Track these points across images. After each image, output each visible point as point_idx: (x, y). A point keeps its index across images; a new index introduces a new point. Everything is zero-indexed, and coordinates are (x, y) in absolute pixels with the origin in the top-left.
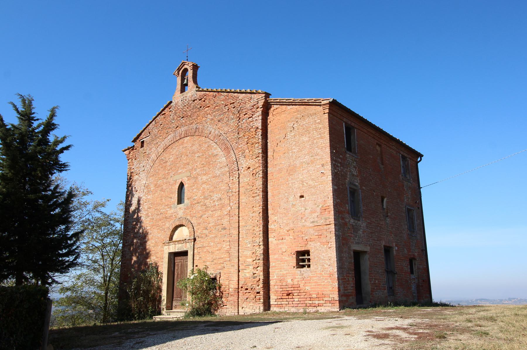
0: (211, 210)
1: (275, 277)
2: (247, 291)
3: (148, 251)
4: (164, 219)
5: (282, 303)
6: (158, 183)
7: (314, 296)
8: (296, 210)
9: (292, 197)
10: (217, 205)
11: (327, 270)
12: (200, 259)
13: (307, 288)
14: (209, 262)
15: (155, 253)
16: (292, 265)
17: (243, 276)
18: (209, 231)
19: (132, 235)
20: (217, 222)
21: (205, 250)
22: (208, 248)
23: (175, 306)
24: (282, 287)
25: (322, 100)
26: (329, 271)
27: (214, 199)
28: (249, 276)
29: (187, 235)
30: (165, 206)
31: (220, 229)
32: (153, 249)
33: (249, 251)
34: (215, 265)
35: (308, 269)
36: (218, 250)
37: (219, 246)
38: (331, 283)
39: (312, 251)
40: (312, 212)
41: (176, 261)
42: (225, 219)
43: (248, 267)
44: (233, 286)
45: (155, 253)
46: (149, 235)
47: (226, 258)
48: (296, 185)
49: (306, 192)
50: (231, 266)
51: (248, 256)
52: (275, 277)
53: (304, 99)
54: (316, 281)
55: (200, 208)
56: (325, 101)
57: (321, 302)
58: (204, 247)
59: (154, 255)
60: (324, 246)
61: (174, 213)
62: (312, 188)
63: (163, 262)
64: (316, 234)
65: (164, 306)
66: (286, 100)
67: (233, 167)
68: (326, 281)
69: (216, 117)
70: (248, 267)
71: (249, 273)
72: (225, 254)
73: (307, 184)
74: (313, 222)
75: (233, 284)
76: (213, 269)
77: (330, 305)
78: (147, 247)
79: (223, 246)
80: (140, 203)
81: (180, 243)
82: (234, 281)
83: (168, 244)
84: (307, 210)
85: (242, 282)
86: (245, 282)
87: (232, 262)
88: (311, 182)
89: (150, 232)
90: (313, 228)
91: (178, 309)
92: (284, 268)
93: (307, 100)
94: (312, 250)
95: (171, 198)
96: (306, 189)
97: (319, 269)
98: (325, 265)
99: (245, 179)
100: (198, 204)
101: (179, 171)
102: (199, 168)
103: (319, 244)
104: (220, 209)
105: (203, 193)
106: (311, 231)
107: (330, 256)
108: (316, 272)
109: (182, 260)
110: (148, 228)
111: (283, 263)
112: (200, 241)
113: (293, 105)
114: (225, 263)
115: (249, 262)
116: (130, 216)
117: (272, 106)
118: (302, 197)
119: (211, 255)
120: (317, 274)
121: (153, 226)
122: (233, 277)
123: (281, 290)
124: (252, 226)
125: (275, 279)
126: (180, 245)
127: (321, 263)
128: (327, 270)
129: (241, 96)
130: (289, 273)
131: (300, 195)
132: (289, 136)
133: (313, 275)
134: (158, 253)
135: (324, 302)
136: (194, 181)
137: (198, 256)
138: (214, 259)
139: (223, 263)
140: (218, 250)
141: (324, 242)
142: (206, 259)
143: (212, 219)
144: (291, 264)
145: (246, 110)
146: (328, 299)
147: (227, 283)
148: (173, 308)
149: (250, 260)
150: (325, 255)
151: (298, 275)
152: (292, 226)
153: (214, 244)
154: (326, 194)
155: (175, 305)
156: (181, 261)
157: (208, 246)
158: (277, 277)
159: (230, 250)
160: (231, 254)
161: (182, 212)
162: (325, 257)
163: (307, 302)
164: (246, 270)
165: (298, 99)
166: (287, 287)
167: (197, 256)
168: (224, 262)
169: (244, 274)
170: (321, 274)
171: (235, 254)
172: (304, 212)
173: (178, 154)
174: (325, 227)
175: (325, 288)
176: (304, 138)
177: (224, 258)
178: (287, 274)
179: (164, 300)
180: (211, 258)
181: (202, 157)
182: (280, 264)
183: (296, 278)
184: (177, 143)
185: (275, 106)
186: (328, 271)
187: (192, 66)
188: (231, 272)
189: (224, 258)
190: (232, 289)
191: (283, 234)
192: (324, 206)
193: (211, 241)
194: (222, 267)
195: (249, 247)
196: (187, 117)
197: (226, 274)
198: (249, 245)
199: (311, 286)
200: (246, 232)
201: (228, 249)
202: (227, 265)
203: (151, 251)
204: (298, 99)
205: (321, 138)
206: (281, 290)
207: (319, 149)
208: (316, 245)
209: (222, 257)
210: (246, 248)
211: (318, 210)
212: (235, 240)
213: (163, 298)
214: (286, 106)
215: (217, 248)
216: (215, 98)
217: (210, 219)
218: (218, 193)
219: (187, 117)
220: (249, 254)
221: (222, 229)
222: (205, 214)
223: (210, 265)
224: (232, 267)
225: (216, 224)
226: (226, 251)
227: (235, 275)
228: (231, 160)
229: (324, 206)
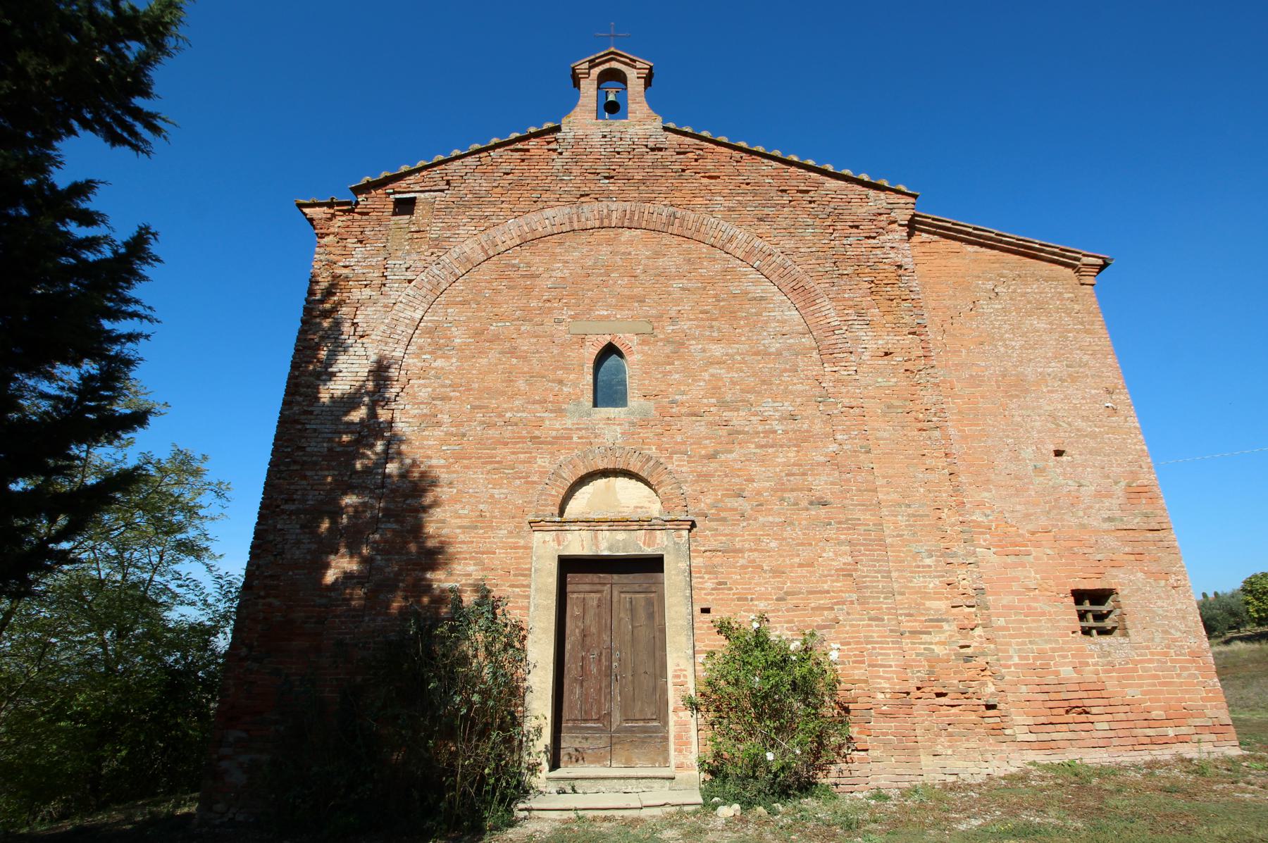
0: (755, 442)
1: (1016, 660)
2: (942, 700)
3: (431, 543)
4: (524, 443)
5: (1055, 736)
6: (492, 328)
7: (1157, 715)
8: (1051, 483)
9: (1030, 450)
10: (780, 432)
11: (1180, 644)
12: (719, 589)
13: (1129, 691)
14: (766, 599)
15: (477, 553)
16: (1067, 628)
17: (922, 654)
18: (755, 504)
19: (329, 479)
20: (789, 481)
21: (741, 562)
22: (756, 554)
23: (574, 753)
24: (1046, 688)
25: (1084, 255)
26: (1188, 648)
27: (766, 414)
28: (948, 655)
29: (637, 507)
30: (528, 403)
31: (804, 503)
32: (461, 537)
33: (930, 577)
34: (794, 611)
35: (1121, 640)
36: (801, 565)
37: (806, 554)
38: (1201, 679)
39: (1125, 592)
40: (1099, 495)
41: (569, 588)
42: (819, 475)
43: (937, 626)
44: (888, 685)
45: (477, 553)
46: (442, 487)
47: (842, 591)
48: (1038, 424)
49: (1072, 444)
50: (870, 619)
51: (930, 593)
52: (1016, 660)
53: (1031, 240)
54: (1154, 672)
55: (702, 429)
56: (1090, 258)
57: (1184, 730)
58: (741, 551)
59: (466, 559)
60: (1158, 583)
61: (580, 429)
62: (1086, 436)
63: (529, 586)
64: (1127, 549)
65: (542, 755)
66: (975, 229)
67: (833, 342)
68: (1185, 674)
69: (748, 209)
70: (937, 626)
71: (943, 643)
72: (837, 581)
73: (1069, 424)
74: (1110, 519)
75: (888, 679)
76: (786, 625)
77: (1213, 737)
78: (430, 529)
79: (824, 555)
80: (388, 379)
81: (623, 528)
82: (891, 666)
83: (560, 528)
84: (1085, 488)
85: (919, 671)
86: (930, 673)
87: (871, 605)
88: (1079, 423)
89: (443, 476)
90: (1113, 534)
91: (592, 762)
92: (1041, 635)
93: (1040, 245)
94: (1123, 590)
95: (561, 382)
96: (1070, 437)
97: (1157, 640)
98: (1173, 631)
99: (880, 380)
100: (694, 418)
101: (597, 313)
102: (691, 320)
103: (1140, 575)
104: (795, 446)
105: (713, 388)
106: (1111, 541)
107: (1181, 610)
108: (1148, 648)
109: (605, 584)
110: (434, 462)
111: (1034, 621)
112: (717, 529)
113: (982, 245)
114: (842, 610)
115: (939, 610)
116: (317, 410)
117: (917, 233)
118: (1059, 453)
119: (774, 578)
120: (1152, 654)
121: (458, 457)
122: (881, 654)
123: (1046, 697)
124: (931, 506)
125: (1016, 665)
126: (621, 536)
127: (1159, 626)
128: (1180, 644)
129: (832, 184)
130: (1062, 649)
131: (1053, 448)
132: (986, 307)
133: (1141, 655)
134: (494, 553)
135: (1193, 730)
136: (668, 349)
137: (712, 576)
138: (787, 593)
139: (832, 609)
140: (801, 565)
141: (1154, 571)
142: (750, 589)
143: (764, 469)
144: (1063, 624)
145: (855, 218)
146: (1202, 722)
147: (858, 673)
148: (564, 758)
149: (942, 605)
150: (1165, 605)
151: (1092, 656)
152: (1043, 522)
153: (781, 545)
154: (1131, 457)
155: (576, 750)
156: (599, 587)
157: (756, 550)
158: (1021, 658)
159: (856, 570)
160: (865, 582)
161: (619, 431)
162: (1167, 611)
163: (1139, 732)
164: (929, 633)
165: (1012, 236)
166: (1059, 688)
167: (706, 576)
168: (837, 603)
169: (922, 646)
170: (1166, 654)
171: (878, 581)
172: (1078, 491)
173: (590, 263)
174: (1150, 534)
175: (1187, 692)
176: (1035, 322)
177: (833, 592)
178: (1053, 650)
179: (539, 731)
180: (773, 588)
181: (701, 292)
182: (1026, 622)
183: (1087, 664)
184: (584, 237)
185: (924, 235)
186: (1186, 647)
187: (647, 71)
188: (872, 637)
189: (833, 592)
190: (888, 696)
191: (1021, 539)
192: (1134, 485)
193: (769, 535)
194: (832, 620)
195: (930, 566)
196: (629, 180)
197: (849, 644)
198: (928, 561)
199: (1141, 686)
200: (907, 521)
201: (844, 564)
202: (848, 614)
203: (450, 543)
204: (1012, 236)
205: (1085, 332)
206: (1046, 697)
207: (1085, 354)
208: (1132, 578)
209: (826, 587)
210: (919, 567)
211: (1119, 490)
212: (870, 540)
213: (529, 725)
214: (959, 243)
215: (797, 560)
216: (738, 164)
217: (754, 468)
218: (779, 399)
219: (629, 180)
220: (931, 585)
221: (811, 503)
222: (731, 452)
223: (773, 611)
224: (874, 623)
225: (783, 484)
226: (837, 570)
227: (890, 648)
228: (822, 323)
229: (1134, 485)
